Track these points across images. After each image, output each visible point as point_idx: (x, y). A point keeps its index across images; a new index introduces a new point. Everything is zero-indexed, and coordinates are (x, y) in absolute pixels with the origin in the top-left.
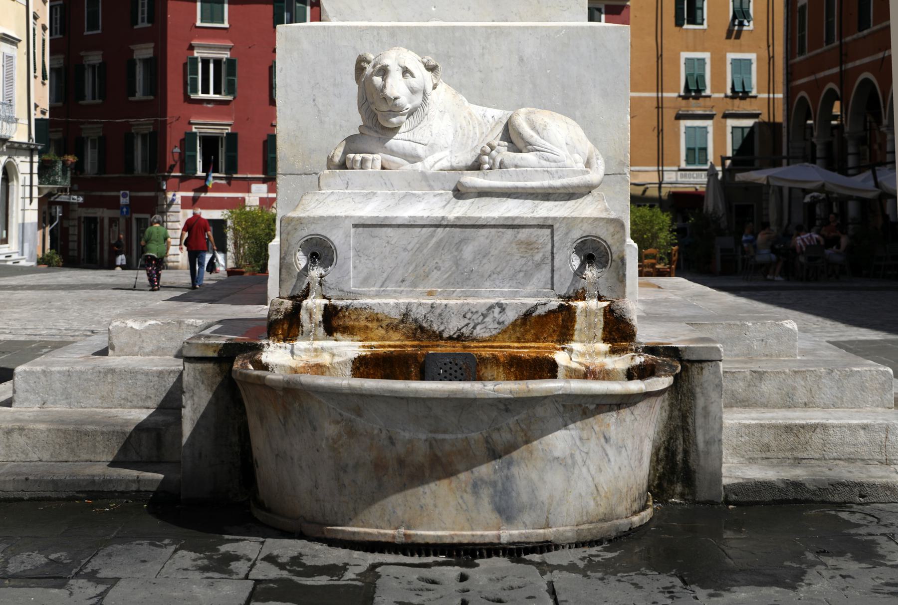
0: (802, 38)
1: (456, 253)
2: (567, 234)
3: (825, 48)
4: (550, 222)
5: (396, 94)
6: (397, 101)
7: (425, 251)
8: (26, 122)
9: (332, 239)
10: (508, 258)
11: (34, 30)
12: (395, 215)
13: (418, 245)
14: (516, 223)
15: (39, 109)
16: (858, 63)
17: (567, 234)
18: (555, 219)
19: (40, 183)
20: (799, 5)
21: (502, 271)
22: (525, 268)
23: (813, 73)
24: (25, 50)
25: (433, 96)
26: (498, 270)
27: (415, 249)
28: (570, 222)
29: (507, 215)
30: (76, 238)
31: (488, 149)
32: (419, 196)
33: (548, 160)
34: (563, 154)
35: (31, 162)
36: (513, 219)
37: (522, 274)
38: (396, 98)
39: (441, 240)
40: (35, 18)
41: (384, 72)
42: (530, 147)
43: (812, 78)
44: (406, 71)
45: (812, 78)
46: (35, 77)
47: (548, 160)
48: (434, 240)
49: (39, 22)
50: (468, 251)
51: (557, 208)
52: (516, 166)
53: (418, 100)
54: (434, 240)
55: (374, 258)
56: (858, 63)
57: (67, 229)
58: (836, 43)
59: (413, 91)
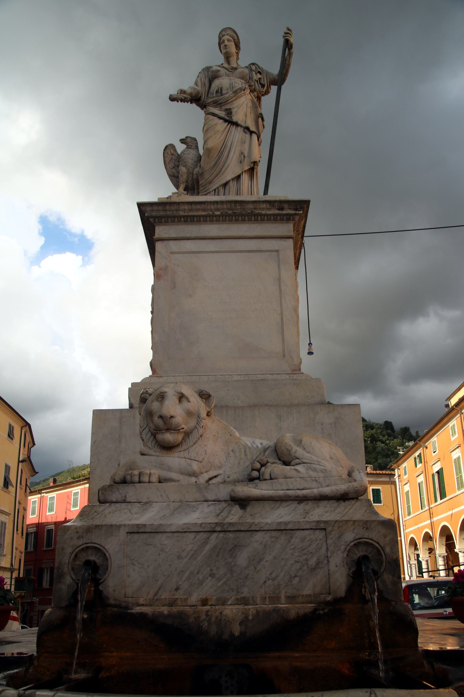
0: (409, 507)
1: (230, 560)
2: (340, 537)
3: (421, 511)
4: (322, 526)
5: (173, 413)
6: (173, 420)
7: (200, 558)
8: (10, 557)
9: (106, 547)
10: (283, 563)
11: (18, 510)
12: (169, 523)
13: (192, 553)
14: (289, 527)
15: (18, 551)
16: (439, 517)
17: (340, 537)
18: (326, 522)
19: (15, 590)
20: (405, 491)
21: (277, 576)
22: (300, 573)
23: (416, 525)
24: (12, 519)
25: (207, 422)
26: (273, 575)
27: (189, 556)
28: (342, 524)
29: (280, 520)
30: (36, 622)
31: (258, 465)
32: (193, 507)
33: (315, 470)
34: (329, 465)
35: (11, 578)
36: (286, 523)
37: (297, 579)
38: (172, 417)
39: (215, 547)
40: (19, 503)
41: (162, 397)
42: (297, 461)
43: (416, 527)
44: (181, 397)
45: (416, 527)
46: (17, 533)
47: (315, 470)
48: (208, 547)
49: (22, 506)
50: (242, 559)
51: (328, 514)
52: (286, 477)
53: (192, 423)
54: (208, 547)
55: (148, 566)
56: (439, 517)
57: (32, 617)
58: (427, 508)
59: (189, 414)
